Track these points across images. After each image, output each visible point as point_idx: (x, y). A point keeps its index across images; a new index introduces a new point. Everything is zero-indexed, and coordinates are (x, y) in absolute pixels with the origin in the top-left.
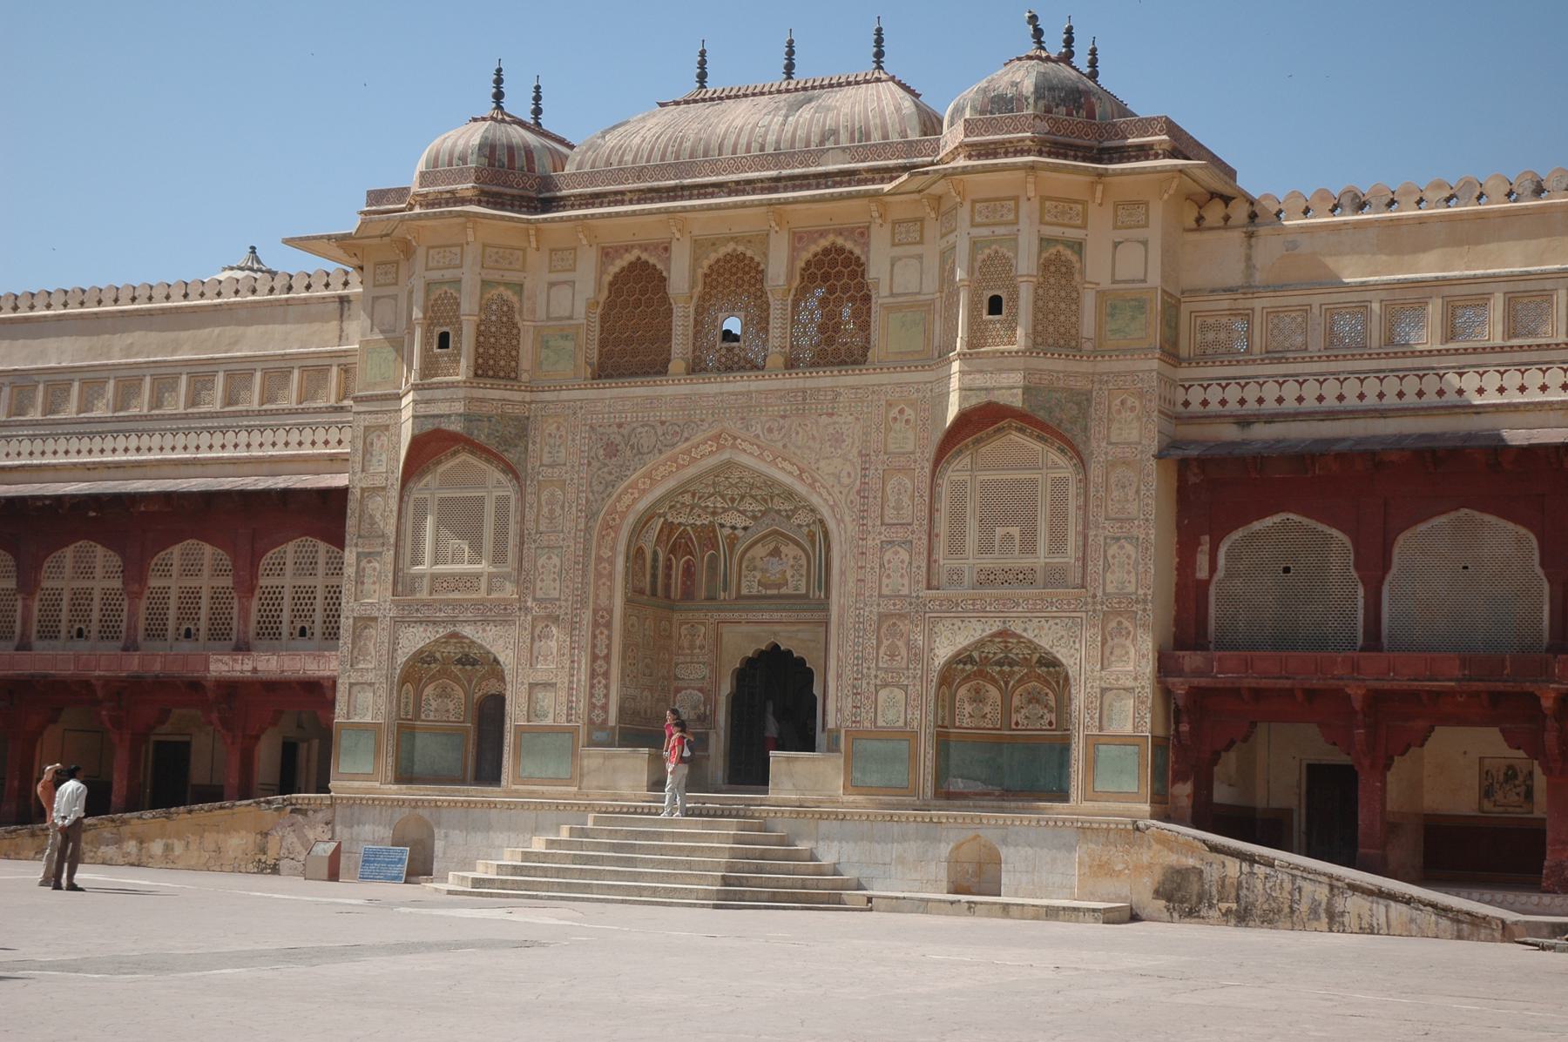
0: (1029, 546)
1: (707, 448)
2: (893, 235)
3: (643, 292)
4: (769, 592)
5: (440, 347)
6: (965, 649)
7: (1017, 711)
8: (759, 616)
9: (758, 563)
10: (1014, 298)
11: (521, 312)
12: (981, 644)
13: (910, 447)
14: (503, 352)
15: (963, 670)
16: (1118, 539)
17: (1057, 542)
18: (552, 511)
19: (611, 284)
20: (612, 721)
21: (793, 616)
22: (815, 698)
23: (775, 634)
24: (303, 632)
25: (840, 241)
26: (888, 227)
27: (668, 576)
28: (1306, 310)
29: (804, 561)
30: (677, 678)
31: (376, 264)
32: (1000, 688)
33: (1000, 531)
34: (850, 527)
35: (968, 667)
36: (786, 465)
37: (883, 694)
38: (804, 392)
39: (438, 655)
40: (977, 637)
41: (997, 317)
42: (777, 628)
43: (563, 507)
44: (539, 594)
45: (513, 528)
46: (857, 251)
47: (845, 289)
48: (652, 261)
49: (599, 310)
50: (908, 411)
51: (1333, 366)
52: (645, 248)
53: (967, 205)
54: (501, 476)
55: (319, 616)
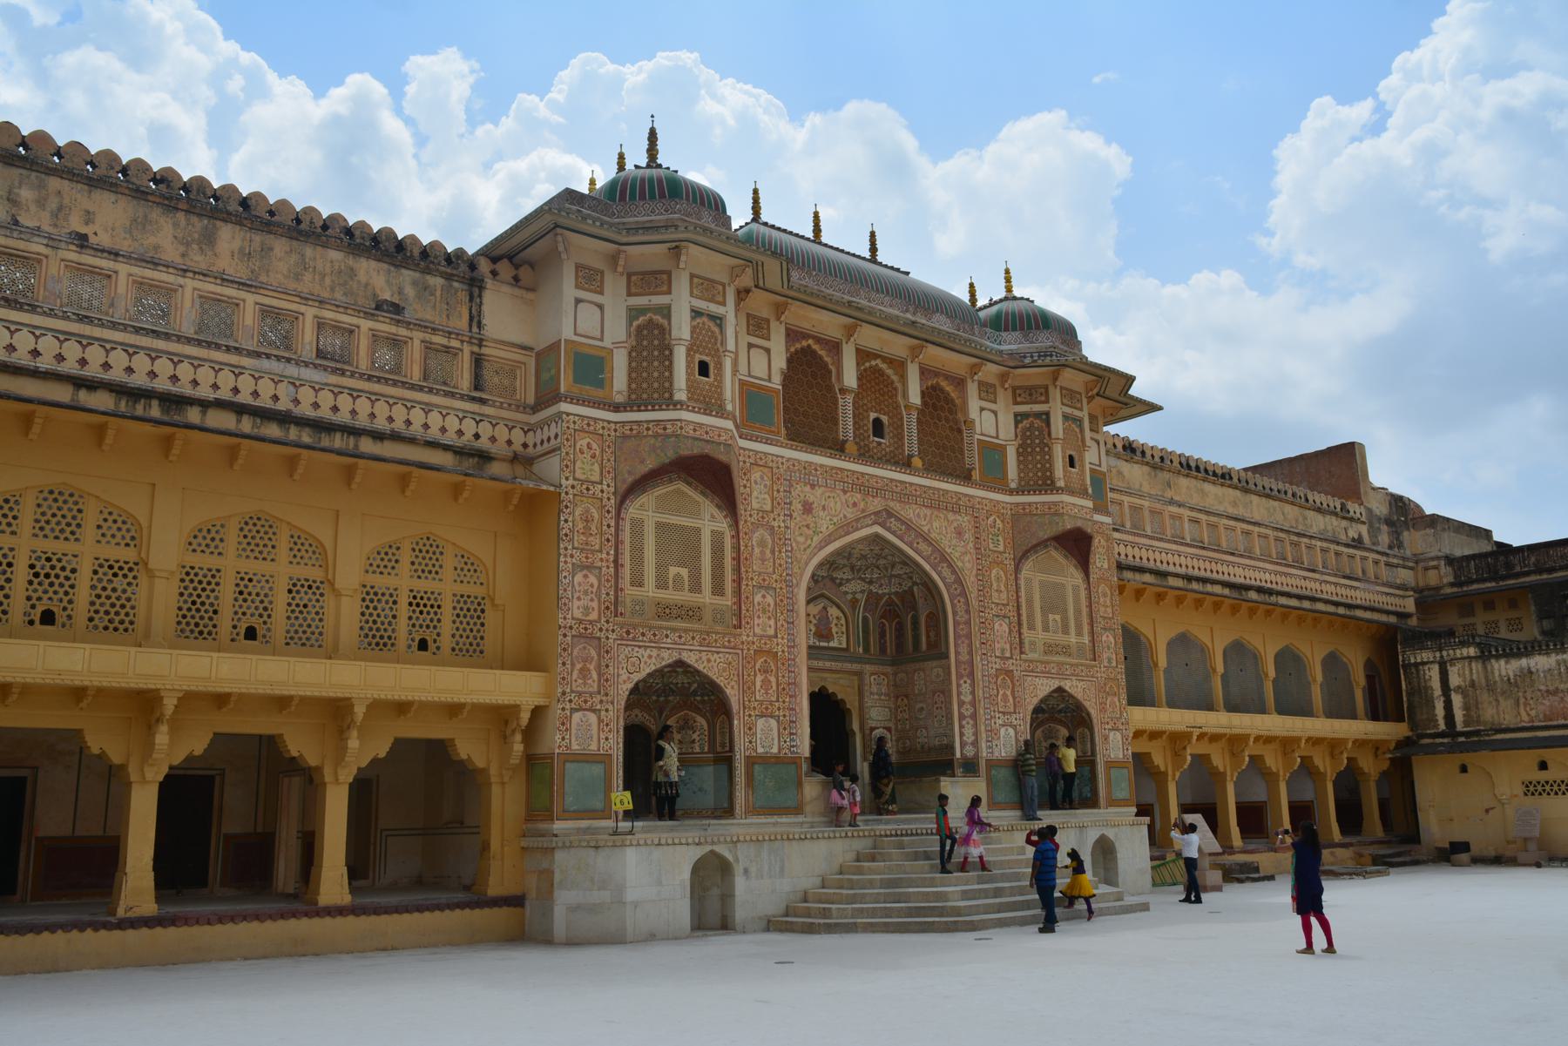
0: (1066, 631)
10: (1082, 460)
13: (1001, 548)
18: (762, 553)
24: (423, 645)
25: (944, 384)
28: (1120, 504)
29: (843, 621)
31: (578, 267)
34: (974, 603)
36: (923, 546)
37: (1003, 730)
44: (758, 630)
51: (1138, 540)
52: (818, 340)
54: (716, 511)
55: (447, 627)
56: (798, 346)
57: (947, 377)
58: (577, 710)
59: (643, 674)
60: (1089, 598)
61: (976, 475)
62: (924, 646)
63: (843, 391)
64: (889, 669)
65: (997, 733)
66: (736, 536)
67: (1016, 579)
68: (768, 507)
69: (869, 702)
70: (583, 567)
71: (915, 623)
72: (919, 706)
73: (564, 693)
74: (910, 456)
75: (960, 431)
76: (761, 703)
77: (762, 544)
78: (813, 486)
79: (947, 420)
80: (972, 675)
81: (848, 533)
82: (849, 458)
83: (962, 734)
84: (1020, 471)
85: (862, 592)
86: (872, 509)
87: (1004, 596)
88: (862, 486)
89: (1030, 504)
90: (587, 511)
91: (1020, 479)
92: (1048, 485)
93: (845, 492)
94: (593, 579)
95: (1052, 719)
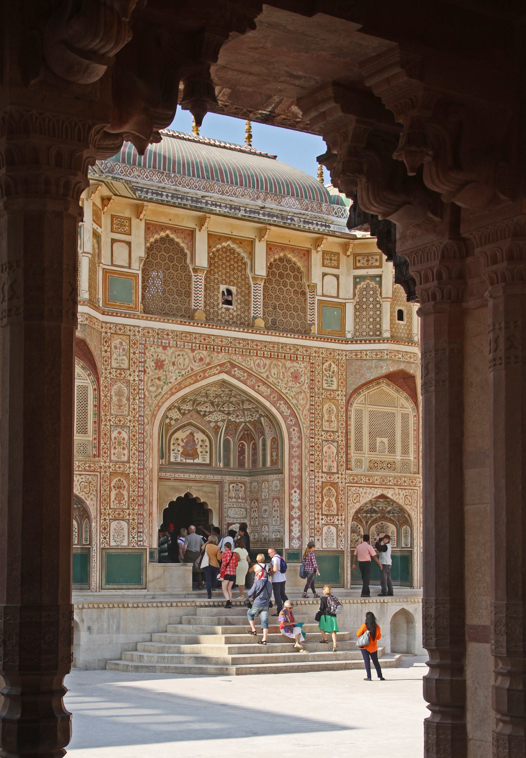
8: (181, 476)
9: (180, 442)
13: (334, 387)
18: (120, 400)
20: (155, 545)
21: (202, 477)
23: (191, 487)
29: (207, 443)
33: (378, 439)
34: (306, 432)
36: (263, 388)
37: (325, 529)
38: (278, 343)
40: (370, 497)
41: (401, 322)
42: (190, 484)
44: (113, 458)
50: (333, 365)
61: (315, 329)
62: (268, 464)
64: (247, 479)
65: (320, 531)
66: (98, 390)
68: (126, 366)
69: (227, 504)
71: (264, 445)
72: (264, 508)
75: (304, 294)
76: (115, 510)
77: (119, 394)
78: (165, 348)
80: (300, 487)
81: (196, 381)
82: (198, 324)
83: (291, 531)
84: (356, 323)
85: (223, 421)
86: (216, 362)
87: (334, 425)
88: (209, 345)
89: (361, 351)
91: (356, 330)
92: (376, 336)
93: (193, 351)
95: (384, 518)
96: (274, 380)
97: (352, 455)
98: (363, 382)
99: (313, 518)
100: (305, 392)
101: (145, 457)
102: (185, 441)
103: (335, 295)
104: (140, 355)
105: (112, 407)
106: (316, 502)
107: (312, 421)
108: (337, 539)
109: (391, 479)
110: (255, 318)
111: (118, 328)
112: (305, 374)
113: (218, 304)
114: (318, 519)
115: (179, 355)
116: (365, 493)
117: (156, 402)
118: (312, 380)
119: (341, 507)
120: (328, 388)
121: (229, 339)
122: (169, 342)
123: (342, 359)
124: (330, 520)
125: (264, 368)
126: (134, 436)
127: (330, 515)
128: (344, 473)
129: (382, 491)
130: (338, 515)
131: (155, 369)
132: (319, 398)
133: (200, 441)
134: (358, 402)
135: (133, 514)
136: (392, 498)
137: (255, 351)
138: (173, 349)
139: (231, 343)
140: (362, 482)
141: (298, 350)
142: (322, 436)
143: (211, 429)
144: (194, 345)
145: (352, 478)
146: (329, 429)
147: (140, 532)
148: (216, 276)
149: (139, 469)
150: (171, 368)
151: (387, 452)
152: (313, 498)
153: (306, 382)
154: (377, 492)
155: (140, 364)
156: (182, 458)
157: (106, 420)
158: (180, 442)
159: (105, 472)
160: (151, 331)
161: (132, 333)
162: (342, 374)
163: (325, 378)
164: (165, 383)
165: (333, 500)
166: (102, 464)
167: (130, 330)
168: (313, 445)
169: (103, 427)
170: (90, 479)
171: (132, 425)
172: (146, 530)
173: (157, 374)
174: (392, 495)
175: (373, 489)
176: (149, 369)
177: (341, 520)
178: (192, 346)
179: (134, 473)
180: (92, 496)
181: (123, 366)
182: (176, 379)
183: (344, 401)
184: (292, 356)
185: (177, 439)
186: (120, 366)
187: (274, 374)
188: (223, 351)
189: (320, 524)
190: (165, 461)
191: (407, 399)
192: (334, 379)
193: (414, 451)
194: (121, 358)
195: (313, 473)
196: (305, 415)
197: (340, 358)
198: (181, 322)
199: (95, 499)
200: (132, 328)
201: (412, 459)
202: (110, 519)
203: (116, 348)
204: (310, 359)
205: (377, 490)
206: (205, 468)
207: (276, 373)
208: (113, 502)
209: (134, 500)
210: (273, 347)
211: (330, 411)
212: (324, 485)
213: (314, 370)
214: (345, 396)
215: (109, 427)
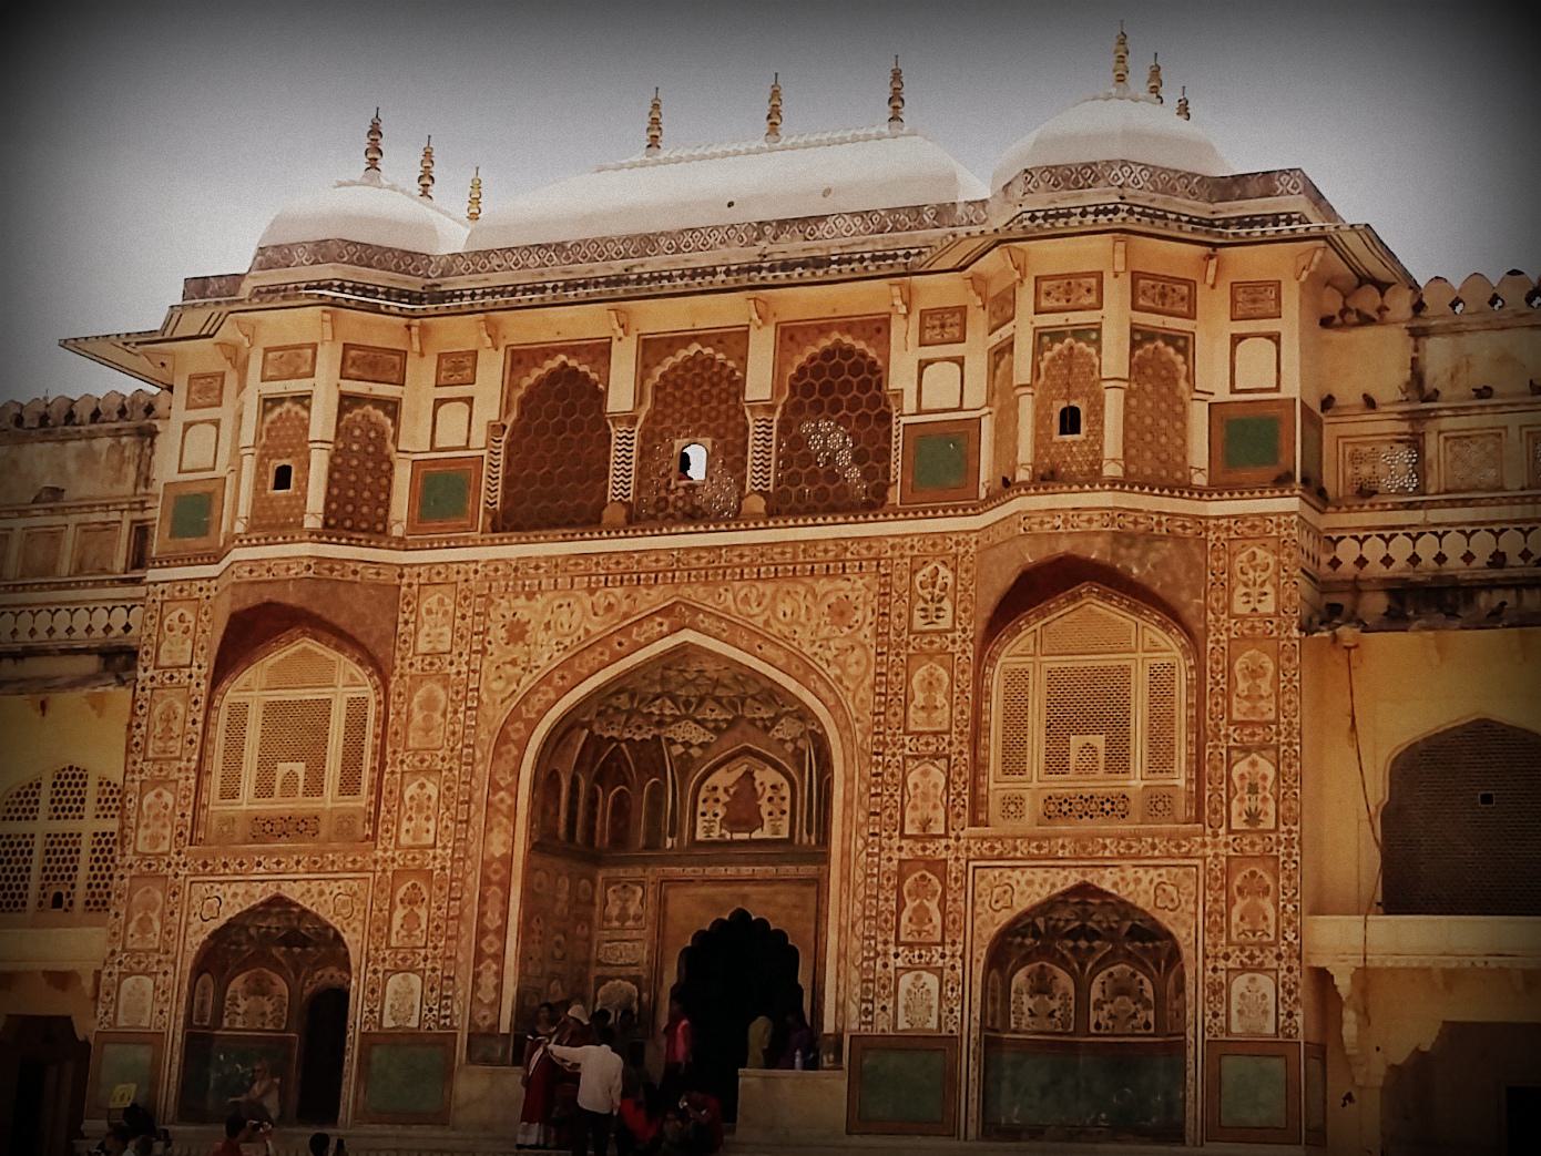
0: (1118, 760)
1: (652, 628)
2: (922, 328)
3: (569, 412)
4: (737, 836)
5: (276, 488)
6: (1026, 914)
7: (1099, 1005)
9: (720, 794)
11: (395, 439)
12: (1049, 906)
13: (945, 623)
14: (366, 494)
15: (1021, 945)
16: (1247, 750)
17: (1161, 759)
19: (523, 402)
22: (800, 990)
23: (745, 897)
25: (848, 340)
26: (915, 318)
27: (592, 816)
29: (786, 792)
30: (599, 963)
32: (1072, 973)
33: (1076, 741)
35: (1029, 941)
36: (768, 650)
39: (253, 931)
40: (1045, 893)
41: (1075, 437)
42: (747, 889)
43: (444, 715)
44: (405, 840)
45: (369, 740)
46: (872, 353)
47: (854, 405)
48: (581, 369)
49: (504, 438)
52: (573, 351)
53: (1029, 283)
54: (355, 669)
56: (536, 373)
57: (848, 326)
58: (128, 975)
59: (223, 921)
60: (1198, 687)
61: (894, 496)
63: (614, 420)
67: (979, 676)
70: (156, 783)
73: (113, 953)
74: (750, 494)
75: (885, 418)
77: (430, 703)
78: (530, 596)
79: (854, 405)
86: (644, 608)
88: (630, 574)
90: (170, 706)
93: (592, 592)
94: (168, 798)
96: (781, 627)
97: (992, 785)
98: (993, 600)
99: (872, 954)
100: (863, 646)
101: (471, 832)
102: (732, 791)
103: (956, 406)
104: (477, 618)
105: (411, 735)
106: (879, 913)
107: (880, 713)
108: (940, 1006)
109: (1108, 841)
110: (750, 494)
111: (434, 571)
112: (865, 604)
113: (669, 483)
114: (886, 954)
115: (561, 606)
116: (1030, 883)
117: (501, 714)
118: (884, 614)
119: (954, 922)
120: (927, 627)
121: (675, 553)
122: (540, 584)
123: (967, 552)
124: (920, 956)
125: (759, 605)
126: (449, 789)
127: (921, 945)
128: (962, 834)
129: (1084, 874)
130: (943, 943)
131: (507, 644)
132: (898, 655)
133: (768, 789)
134: (1017, 650)
135: (434, 958)
136: (1114, 891)
137: (738, 571)
138: (550, 595)
139: (678, 560)
140: (1019, 855)
141: (846, 549)
142: (903, 746)
143: (790, 758)
144: (594, 579)
145: (986, 845)
146: (926, 729)
147: (447, 997)
148: (668, 423)
149: (452, 859)
150: (542, 636)
151: (1101, 770)
152: (874, 902)
153: (868, 621)
154: (1066, 878)
155: (475, 638)
156: (723, 831)
157: (393, 763)
158: (720, 794)
159: (384, 871)
160: (500, 567)
161: (462, 577)
162: (966, 590)
163: (921, 604)
164: (523, 669)
165: (933, 905)
166: (380, 853)
167: (458, 572)
168: (880, 769)
169: (386, 777)
170: (356, 888)
171: (447, 767)
172: (461, 993)
173: (510, 652)
174: (1115, 885)
175: (1054, 870)
176: (494, 646)
177: (953, 956)
178: (589, 582)
179: (443, 868)
180: (356, 924)
181: (441, 648)
182: (550, 658)
183: (971, 656)
184: (832, 565)
185: (715, 789)
186: (434, 648)
187: (785, 615)
188: (660, 581)
189: (891, 969)
190: (680, 841)
191: (1164, 627)
192: (946, 604)
193: (1188, 763)
194: (439, 630)
195: (877, 839)
196: (862, 700)
197: (962, 550)
198: (564, 535)
199: (360, 929)
200: (463, 566)
201: (1181, 783)
202: (386, 971)
203: (429, 612)
204: (878, 565)
205: (1066, 873)
206: (781, 849)
207: (793, 612)
208: (397, 933)
209: (437, 927)
210: (783, 553)
211: (930, 683)
212: (906, 867)
213: (888, 590)
214: (972, 640)
215: (399, 776)
